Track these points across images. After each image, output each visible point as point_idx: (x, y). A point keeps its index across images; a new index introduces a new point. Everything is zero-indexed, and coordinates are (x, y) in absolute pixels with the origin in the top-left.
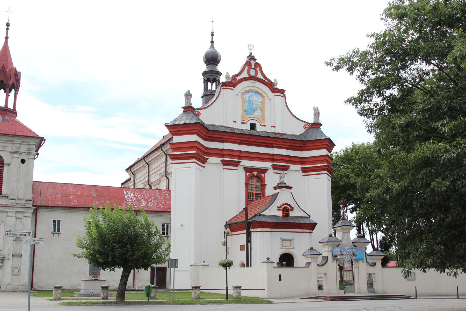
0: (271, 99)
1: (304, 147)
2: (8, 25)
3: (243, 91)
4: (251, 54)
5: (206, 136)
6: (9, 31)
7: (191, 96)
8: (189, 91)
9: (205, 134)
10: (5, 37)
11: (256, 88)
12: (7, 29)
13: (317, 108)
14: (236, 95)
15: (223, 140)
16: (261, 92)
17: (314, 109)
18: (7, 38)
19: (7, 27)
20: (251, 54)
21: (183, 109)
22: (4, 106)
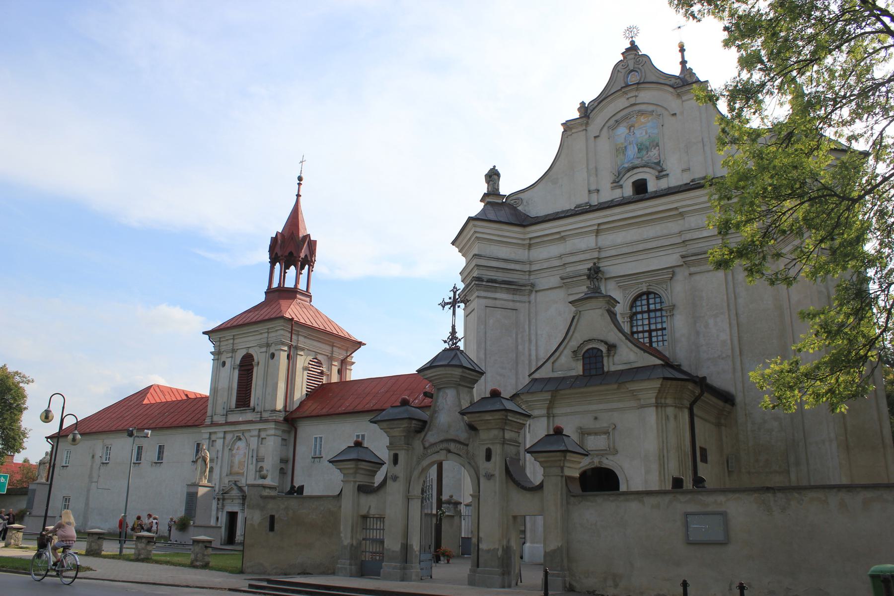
0: (674, 115)
2: (300, 179)
3: (612, 122)
4: (632, 43)
5: (524, 239)
6: (302, 187)
8: (495, 166)
9: (521, 236)
10: (296, 195)
12: (299, 184)
14: (595, 137)
15: (562, 236)
16: (651, 108)
18: (298, 196)
19: (299, 182)
20: (632, 43)
22: (293, 287)
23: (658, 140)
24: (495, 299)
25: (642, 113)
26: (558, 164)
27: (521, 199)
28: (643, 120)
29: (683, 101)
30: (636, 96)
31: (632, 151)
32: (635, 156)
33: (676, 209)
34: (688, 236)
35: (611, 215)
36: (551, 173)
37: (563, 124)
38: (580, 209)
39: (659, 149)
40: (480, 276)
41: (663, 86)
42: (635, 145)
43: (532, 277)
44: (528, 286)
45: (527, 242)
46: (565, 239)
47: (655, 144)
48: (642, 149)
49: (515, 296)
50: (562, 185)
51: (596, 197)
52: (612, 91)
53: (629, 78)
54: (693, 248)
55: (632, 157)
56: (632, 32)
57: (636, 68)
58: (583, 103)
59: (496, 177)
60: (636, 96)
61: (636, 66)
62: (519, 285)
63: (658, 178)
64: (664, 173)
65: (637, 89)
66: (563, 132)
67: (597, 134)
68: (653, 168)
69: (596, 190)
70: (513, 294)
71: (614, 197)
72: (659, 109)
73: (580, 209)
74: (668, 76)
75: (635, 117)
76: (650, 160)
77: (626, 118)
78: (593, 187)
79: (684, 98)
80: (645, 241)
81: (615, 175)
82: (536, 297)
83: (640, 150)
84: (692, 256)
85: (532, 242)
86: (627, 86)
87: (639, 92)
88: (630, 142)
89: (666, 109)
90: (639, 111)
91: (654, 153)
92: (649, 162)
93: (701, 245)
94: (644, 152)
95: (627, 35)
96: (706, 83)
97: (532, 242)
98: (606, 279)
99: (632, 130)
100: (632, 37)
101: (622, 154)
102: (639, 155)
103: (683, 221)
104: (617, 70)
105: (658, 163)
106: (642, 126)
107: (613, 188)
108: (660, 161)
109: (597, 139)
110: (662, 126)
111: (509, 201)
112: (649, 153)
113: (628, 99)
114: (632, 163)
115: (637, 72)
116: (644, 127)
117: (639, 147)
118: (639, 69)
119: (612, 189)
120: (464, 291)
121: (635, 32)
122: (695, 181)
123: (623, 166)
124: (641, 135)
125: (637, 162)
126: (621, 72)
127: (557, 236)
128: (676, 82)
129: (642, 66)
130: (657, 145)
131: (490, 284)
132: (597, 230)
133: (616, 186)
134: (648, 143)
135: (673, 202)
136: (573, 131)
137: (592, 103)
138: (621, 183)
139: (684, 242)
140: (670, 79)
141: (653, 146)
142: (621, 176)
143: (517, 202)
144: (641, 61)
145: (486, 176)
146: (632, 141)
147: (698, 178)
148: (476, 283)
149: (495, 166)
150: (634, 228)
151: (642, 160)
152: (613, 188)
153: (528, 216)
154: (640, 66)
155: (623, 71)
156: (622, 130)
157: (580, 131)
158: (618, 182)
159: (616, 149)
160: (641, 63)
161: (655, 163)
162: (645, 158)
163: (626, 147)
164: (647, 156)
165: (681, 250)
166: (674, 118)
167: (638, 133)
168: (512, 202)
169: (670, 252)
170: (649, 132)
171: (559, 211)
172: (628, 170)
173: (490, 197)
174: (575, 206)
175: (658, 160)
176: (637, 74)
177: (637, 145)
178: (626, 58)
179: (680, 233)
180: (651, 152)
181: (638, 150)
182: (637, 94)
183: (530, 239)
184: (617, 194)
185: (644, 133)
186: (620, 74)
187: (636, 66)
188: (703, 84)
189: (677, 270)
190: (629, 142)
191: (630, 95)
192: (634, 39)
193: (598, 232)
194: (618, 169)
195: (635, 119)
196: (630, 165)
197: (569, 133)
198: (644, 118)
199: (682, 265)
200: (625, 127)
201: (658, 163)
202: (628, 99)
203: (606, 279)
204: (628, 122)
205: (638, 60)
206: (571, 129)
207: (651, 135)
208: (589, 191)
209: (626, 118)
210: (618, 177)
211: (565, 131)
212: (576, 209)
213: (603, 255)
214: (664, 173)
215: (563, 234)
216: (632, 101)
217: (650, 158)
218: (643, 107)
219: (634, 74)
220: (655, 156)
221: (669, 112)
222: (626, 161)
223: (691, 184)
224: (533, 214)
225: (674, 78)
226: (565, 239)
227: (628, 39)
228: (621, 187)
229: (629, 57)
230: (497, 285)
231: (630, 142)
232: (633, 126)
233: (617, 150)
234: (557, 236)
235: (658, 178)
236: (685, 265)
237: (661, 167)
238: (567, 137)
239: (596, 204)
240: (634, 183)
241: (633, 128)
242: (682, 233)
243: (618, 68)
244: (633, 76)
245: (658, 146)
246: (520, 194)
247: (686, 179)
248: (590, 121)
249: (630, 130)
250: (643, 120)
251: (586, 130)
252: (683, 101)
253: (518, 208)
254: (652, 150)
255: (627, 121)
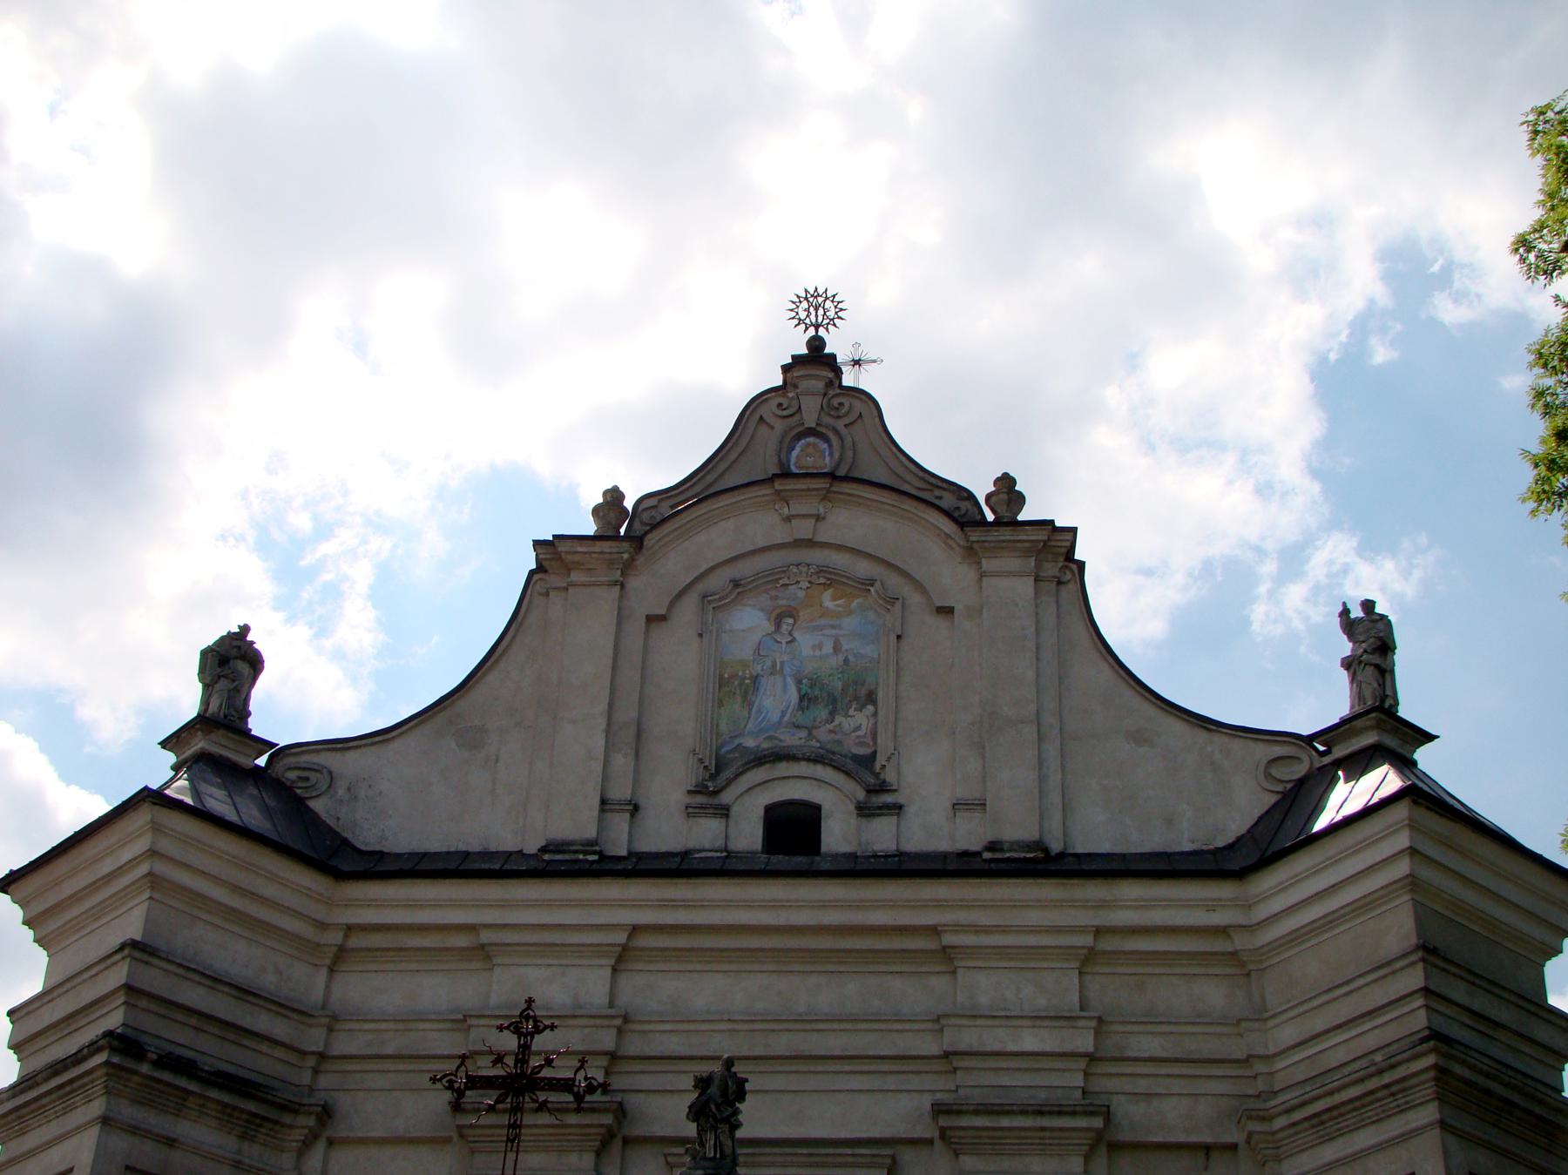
0: (946, 611)
1: (1249, 928)
4: (816, 344)
5: (322, 926)
7: (255, 662)
8: (245, 629)
9: (319, 912)
11: (826, 552)
13: (1368, 605)
14: (651, 619)
15: (482, 947)
16: (863, 568)
17: (1349, 625)
20: (816, 344)
21: (171, 758)
23: (877, 684)
24: (171, 1142)
25: (830, 578)
26: (492, 678)
27: (330, 773)
28: (828, 603)
29: (982, 575)
30: (818, 518)
31: (776, 700)
32: (786, 719)
33: (934, 931)
34: (968, 1038)
35: (688, 905)
36: (462, 705)
37: (537, 544)
38: (558, 857)
39: (875, 714)
40: (129, 1032)
41: (922, 506)
42: (790, 681)
43: (324, 1081)
44: (310, 1114)
45: (335, 938)
46: (488, 958)
47: (863, 692)
48: (816, 698)
49: (246, 1146)
50: (497, 761)
51: (626, 827)
52: (731, 481)
53: (795, 453)
54: (977, 1082)
55: (775, 717)
56: (821, 311)
57: (827, 427)
58: (614, 497)
59: (243, 667)
60: (818, 518)
61: (827, 420)
62: (273, 1104)
63: (865, 811)
64: (888, 798)
65: (826, 497)
66: (532, 573)
67: (662, 611)
68: (848, 774)
69: (629, 803)
70: (243, 1137)
71: (692, 844)
72: (894, 581)
73: (558, 857)
74: (932, 480)
75: (804, 585)
76: (839, 742)
77: (774, 579)
78: (621, 791)
79: (987, 565)
80: (807, 1021)
81: (706, 767)
82: (326, 1161)
83: (806, 701)
84: (977, 1113)
85: (356, 941)
86: (786, 474)
87: (829, 505)
88: (774, 666)
89: (918, 585)
90: (821, 570)
91: (856, 722)
92: (837, 749)
93: (1006, 1080)
94: (822, 713)
95: (803, 315)
96: (1069, 536)
97: (356, 941)
98: (627, 1141)
99: (784, 628)
100: (817, 327)
101: (739, 700)
102: (801, 718)
103: (946, 979)
104: (757, 416)
105: (868, 761)
106: (823, 622)
107: (691, 812)
108: (874, 754)
109: (653, 625)
110: (899, 637)
111: (278, 768)
112: (839, 719)
113: (788, 519)
114: (770, 738)
115: (826, 440)
116: (833, 627)
117: (805, 689)
118: (837, 432)
119: (689, 815)
120: (30, 1088)
121: (831, 314)
122: (1002, 850)
123: (737, 742)
124: (818, 653)
125: (793, 739)
126: (772, 428)
127: (462, 941)
128: (958, 508)
129: (846, 426)
130: (871, 698)
131: (167, 1076)
132: (625, 948)
133: (703, 807)
134: (839, 685)
135: (924, 905)
136: (575, 577)
137: (652, 502)
138: (726, 797)
139: (947, 1055)
140: (938, 493)
141: (856, 698)
142: (727, 774)
143: (313, 781)
144: (843, 411)
145: (205, 654)
146: (782, 663)
147: (1012, 843)
148: (116, 1060)
149: (245, 629)
150: (756, 967)
151: (810, 736)
152: (691, 812)
153: (345, 842)
154: (840, 425)
155: (780, 426)
156: (749, 621)
157: (600, 584)
158: (716, 793)
159: (721, 677)
160: (845, 416)
161: (856, 759)
162: (823, 734)
163: (755, 679)
164: (830, 727)
165: (929, 1082)
166: (940, 623)
167: (806, 642)
168: (292, 775)
169: (890, 1082)
170: (845, 647)
171: (470, 850)
172: (760, 759)
173: (213, 736)
174: (544, 843)
175: (867, 751)
176: (826, 446)
177: (799, 682)
178: (796, 386)
179: (938, 1021)
180: (847, 716)
181: (802, 698)
182: (822, 510)
183: (350, 929)
184: (705, 834)
185: (828, 648)
186: (763, 431)
187: (827, 420)
188: (1059, 536)
189: (907, 1155)
190: (769, 663)
191: (798, 507)
192: (822, 332)
193: (622, 958)
194: (719, 748)
195: (801, 594)
196: (765, 745)
197: (554, 580)
198: (834, 599)
199: (930, 1142)
200: (762, 610)
201: (868, 761)
202: (788, 519)
203: (627, 1141)
204: (776, 598)
205: (835, 402)
206: (568, 569)
207: (851, 658)
208: (603, 802)
209: (774, 579)
210: (713, 777)
211: (540, 568)
212: (547, 857)
213: (634, 1046)
214: (888, 798)
215: (486, 937)
216: (804, 529)
217: (837, 737)
218: (838, 560)
219: (814, 445)
220: (859, 733)
221: (929, 598)
222: (750, 725)
223: (987, 855)
224: (368, 836)
225: (953, 492)
226: (488, 958)
227: (803, 327)
228: (724, 812)
229: (805, 384)
230: (193, 1086)
231: (774, 666)
232: (791, 613)
233: (722, 682)
234: (462, 941)
235: (865, 811)
236: (938, 1144)
237: (877, 775)
238: (547, 594)
239: (624, 853)
240: (769, 809)
241: (790, 621)
242: (944, 1021)
243: (761, 411)
244: (811, 450)
245: (874, 702)
246: (328, 754)
247: (968, 835)
248: (641, 559)
249: (778, 625)
250: (828, 603)
251: (622, 586)
252: (982, 575)
253: (313, 804)
254: (851, 712)
255: (773, 593)
